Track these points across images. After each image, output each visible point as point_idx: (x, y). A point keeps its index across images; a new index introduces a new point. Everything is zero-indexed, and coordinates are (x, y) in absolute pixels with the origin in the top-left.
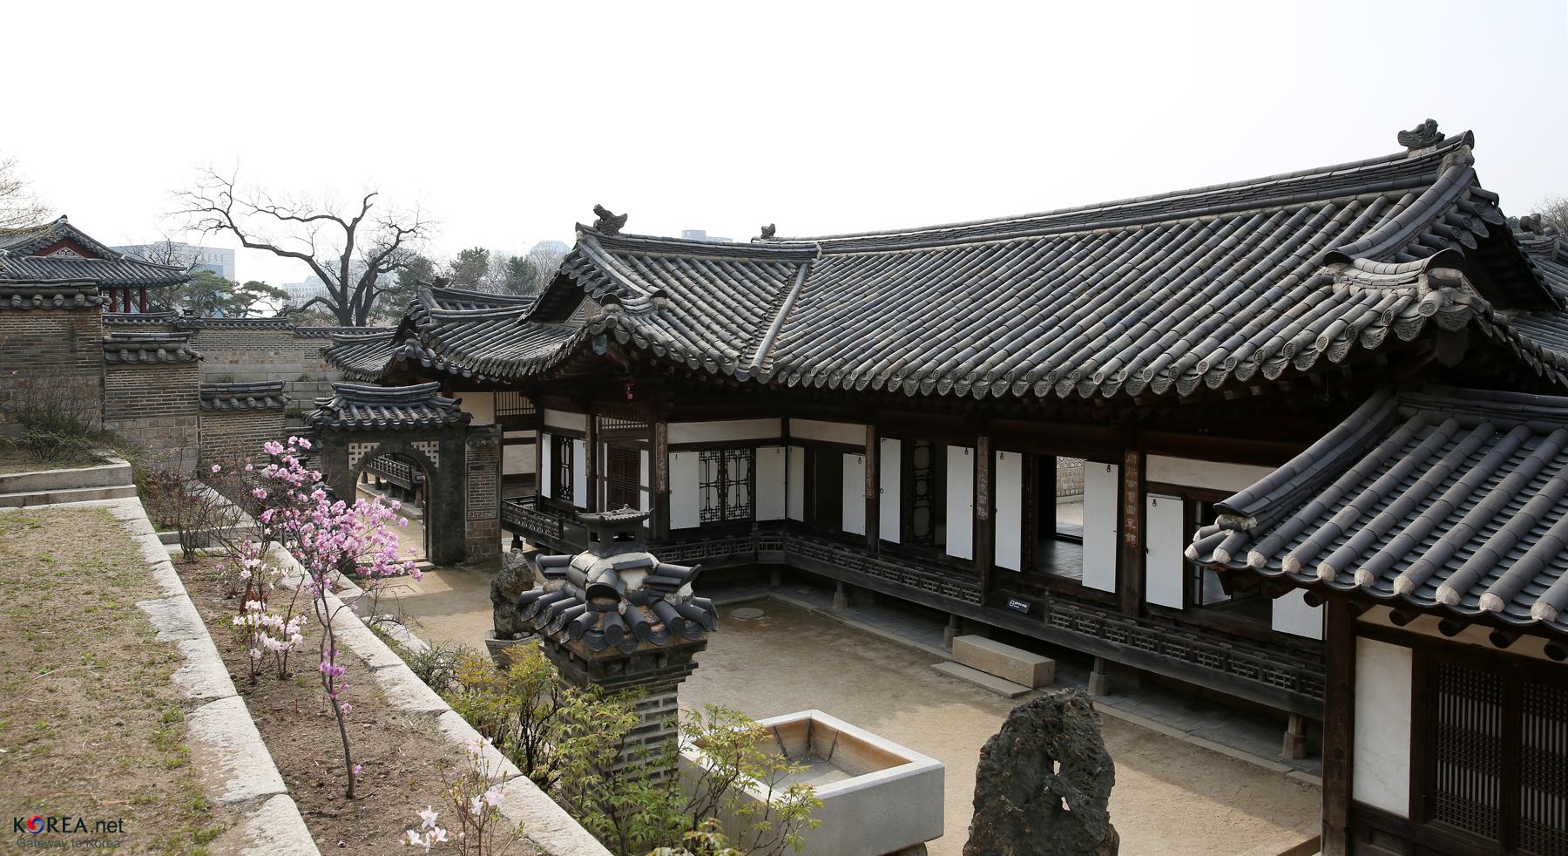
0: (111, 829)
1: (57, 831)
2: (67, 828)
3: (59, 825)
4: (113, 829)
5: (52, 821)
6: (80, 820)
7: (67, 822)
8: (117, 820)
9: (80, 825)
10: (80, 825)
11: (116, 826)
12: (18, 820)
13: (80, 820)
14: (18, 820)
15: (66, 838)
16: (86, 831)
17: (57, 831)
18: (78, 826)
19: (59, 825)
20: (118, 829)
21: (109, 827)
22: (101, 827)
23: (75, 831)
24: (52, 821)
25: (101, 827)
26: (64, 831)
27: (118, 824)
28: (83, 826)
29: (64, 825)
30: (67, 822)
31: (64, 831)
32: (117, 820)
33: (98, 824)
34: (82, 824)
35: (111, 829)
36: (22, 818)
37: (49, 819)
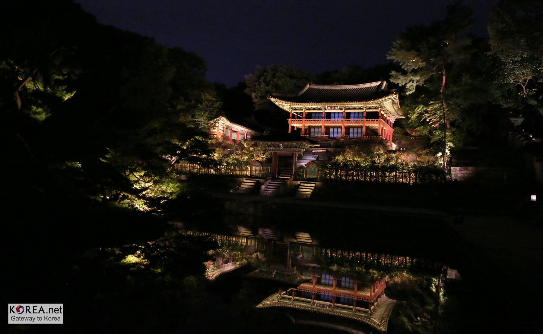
0: (56, 312)
1: (30, 313)
2: (35, 311)
3: (31, 310)
4: (57, 312)
5: (28, 308)
6: (41, 307)
7: (35, 308)
8: (59, 308)
9: (41, 309)
10: (41, 309)
11: (58, 310)
12: (11, 308)
13: (41, 307)
14: (11, 308)
15: (33, 315)
16: (44, 313)
17: (30, 313)
18: (40, 310)
19: (31, 310)
20: (59, 311)
21: (55, 310)
22: (51, 310)
23: (39, 313)
24: (28, 308)
25: (51, 310)
26: (34, 313)
27: (59, 309)
28: (43, 310)
29: (34, 310)
30: (35, 308)
31: (34, 313)
32: (59, 308)
33: (50, 309)
34: (42, 309)
35: (56, 311)
36: (14, 307)
37: (26, 307)
